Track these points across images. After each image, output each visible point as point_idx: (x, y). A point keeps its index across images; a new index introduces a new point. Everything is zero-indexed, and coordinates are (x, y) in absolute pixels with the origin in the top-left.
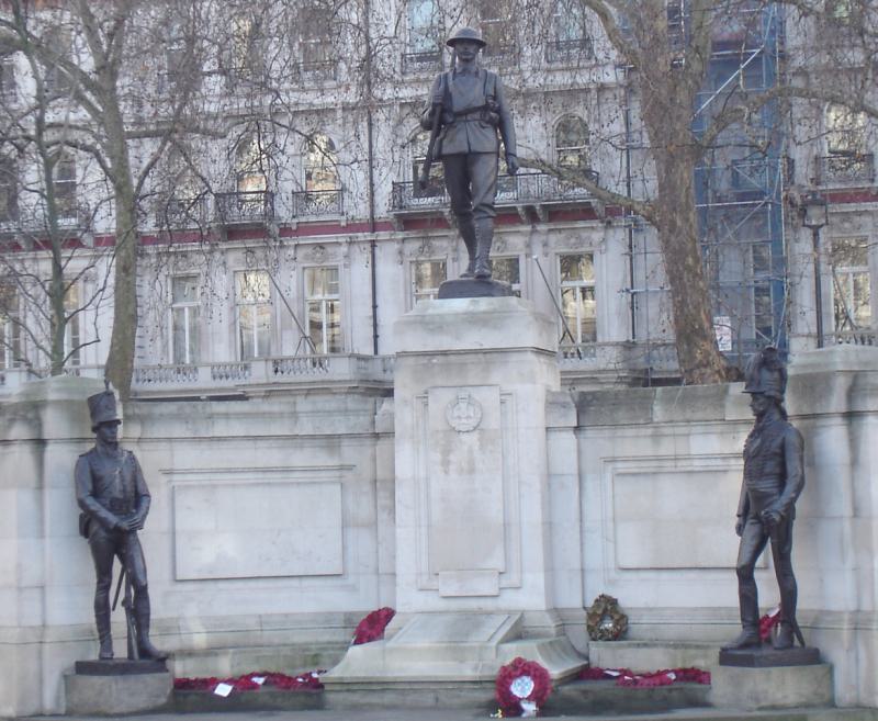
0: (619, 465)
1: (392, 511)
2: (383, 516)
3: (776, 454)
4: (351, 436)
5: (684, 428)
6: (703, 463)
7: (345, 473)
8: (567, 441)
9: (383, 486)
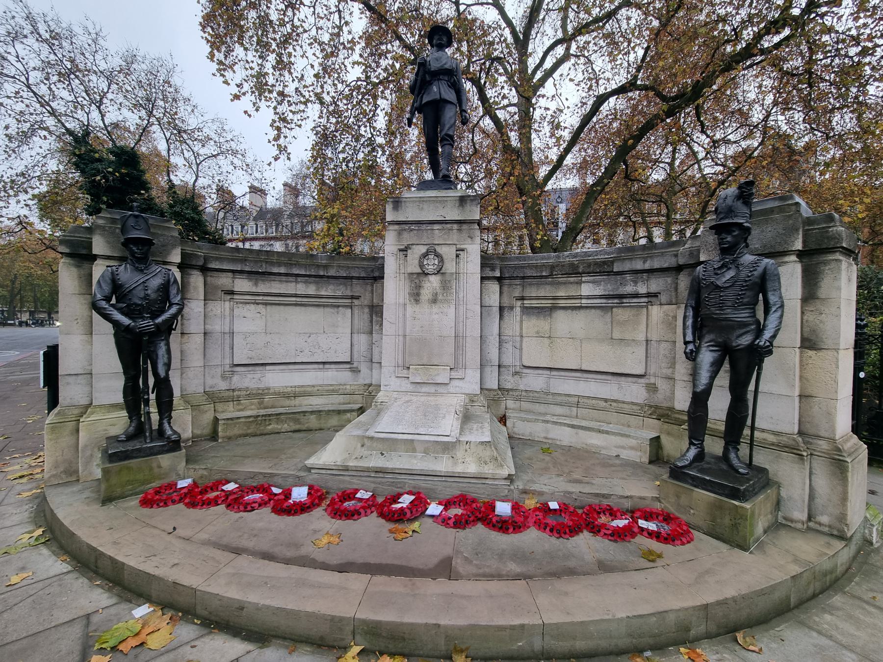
0: (525, 302)
1: (381, 325)
2: (376, 327)
3: (755, 283)
4: (358, 278)
6: (589, 301)
7: (354, 301)
8: (494, 287)
9: (376, 310)
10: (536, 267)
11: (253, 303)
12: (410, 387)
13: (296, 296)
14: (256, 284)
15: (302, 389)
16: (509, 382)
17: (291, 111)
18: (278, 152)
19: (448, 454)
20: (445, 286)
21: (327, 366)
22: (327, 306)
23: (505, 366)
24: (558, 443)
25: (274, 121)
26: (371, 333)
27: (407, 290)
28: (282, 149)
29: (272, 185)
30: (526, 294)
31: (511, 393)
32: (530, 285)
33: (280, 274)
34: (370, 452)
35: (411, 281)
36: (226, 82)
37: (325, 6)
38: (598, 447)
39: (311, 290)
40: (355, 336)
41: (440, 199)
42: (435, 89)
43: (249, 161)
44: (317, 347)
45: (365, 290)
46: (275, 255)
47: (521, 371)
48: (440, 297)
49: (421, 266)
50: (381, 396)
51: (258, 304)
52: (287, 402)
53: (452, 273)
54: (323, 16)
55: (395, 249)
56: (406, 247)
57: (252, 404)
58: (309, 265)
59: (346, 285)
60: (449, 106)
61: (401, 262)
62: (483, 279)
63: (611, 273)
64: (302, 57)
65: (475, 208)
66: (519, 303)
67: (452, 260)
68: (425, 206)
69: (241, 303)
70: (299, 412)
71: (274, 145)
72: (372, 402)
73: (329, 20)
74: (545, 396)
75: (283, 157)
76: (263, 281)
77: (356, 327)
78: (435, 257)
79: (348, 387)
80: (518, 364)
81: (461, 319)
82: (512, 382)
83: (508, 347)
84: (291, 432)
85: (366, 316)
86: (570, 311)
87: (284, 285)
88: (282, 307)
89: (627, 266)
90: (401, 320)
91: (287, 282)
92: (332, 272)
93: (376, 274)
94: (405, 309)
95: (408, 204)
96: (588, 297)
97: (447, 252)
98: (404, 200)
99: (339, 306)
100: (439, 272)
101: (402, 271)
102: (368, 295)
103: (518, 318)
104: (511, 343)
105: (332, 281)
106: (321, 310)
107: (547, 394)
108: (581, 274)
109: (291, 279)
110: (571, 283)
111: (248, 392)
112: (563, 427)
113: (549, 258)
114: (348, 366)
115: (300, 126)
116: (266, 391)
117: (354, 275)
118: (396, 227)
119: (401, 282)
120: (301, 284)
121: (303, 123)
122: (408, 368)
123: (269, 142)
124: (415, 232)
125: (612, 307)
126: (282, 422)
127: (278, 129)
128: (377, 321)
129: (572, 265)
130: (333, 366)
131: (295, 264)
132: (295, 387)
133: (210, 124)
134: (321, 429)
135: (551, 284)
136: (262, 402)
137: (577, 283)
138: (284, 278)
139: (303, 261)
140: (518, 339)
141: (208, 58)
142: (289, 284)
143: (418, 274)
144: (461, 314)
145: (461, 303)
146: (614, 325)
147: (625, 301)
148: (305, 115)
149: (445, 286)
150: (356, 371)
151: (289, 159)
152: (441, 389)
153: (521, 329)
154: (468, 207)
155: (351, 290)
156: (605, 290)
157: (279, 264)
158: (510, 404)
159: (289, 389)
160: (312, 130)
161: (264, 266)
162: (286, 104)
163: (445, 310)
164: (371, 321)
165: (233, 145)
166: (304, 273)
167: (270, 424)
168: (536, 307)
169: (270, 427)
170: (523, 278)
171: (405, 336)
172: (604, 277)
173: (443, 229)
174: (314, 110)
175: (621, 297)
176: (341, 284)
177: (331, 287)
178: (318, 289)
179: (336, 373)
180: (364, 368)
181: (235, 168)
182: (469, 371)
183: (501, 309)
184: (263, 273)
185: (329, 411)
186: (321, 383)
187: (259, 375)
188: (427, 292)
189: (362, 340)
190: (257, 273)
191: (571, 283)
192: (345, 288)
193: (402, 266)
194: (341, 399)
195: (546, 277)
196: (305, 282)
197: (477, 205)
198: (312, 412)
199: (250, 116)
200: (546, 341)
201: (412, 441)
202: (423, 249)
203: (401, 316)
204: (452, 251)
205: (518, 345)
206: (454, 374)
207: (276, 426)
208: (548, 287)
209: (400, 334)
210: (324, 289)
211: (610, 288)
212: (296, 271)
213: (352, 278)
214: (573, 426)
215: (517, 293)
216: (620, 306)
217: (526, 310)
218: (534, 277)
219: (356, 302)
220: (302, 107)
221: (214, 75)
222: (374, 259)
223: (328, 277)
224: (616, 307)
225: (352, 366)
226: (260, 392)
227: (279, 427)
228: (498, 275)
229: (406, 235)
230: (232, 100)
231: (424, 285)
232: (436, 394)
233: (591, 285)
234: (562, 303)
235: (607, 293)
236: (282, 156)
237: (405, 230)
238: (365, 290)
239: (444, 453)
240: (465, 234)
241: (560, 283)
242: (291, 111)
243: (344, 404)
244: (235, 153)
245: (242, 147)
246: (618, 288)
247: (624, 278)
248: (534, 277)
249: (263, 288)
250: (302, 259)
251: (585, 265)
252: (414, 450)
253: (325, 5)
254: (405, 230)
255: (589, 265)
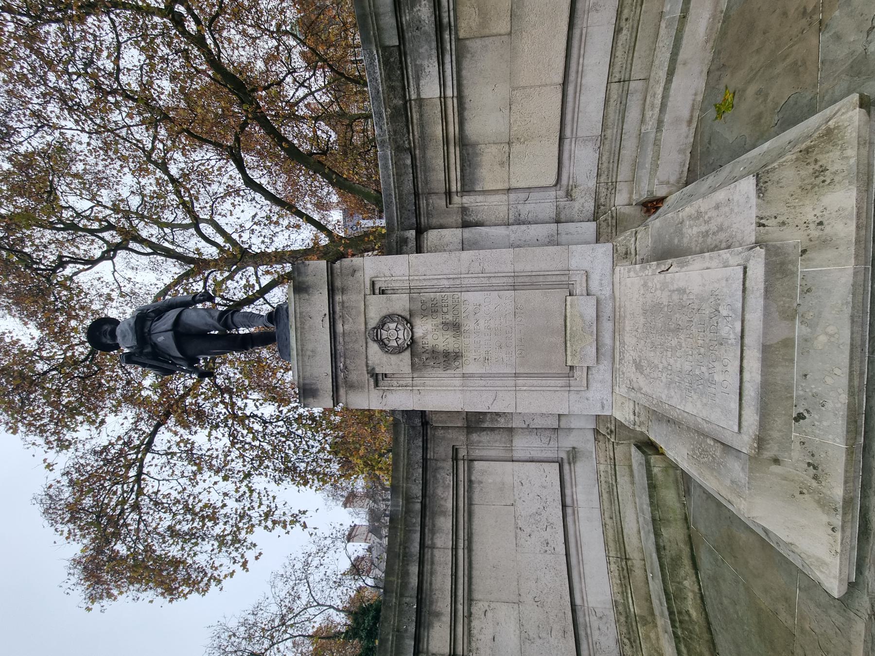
0: (454, 189)
1: (497, 414)
2: (502, 423)
4: (425, 449)
5: (414, 110)
6: (449, 83)
7: (460, 456)
8: (432, 236)
10: (399, 175)
11: (470, 622)
12: (605, 365)
13: (455, 549)
14: (438, 615)
15: (611, 544)
16: (584, 203)
17: (259, 507)
18: (298, 524)
19: (794, 263)
20: (431, 310)
21: (568, 501)
22: (470, 499)
23: (558, 214)
24: (700, 98)
25: (266, 527)
26: (511, 430)
27: (440, 372)
28: (295, 520)
29: (338, 527)
30: (441, 187)
31: (602, 200)
32: (427, 184)
33: (421, 574)
34: (796, 446)
35: (425, 366)
36: (232, 574)
37: (161, 468)
38: (714, 16)
39: (445, 523)
40: (517, 455)
41: (298, 325)
42: (161, 339)
43: (314, 550)
44: (538, 518)
45: (443, 438)
46: (391, 579)
47: (564, 188)
48: (450, 317)
49: (399, 350)
50: (624, 414)
51: (470, 614)
52: (638, 573)
53: (411, 299)
54: (171, 471)
55: (375, 394)
56: (372, 376)
57: (647, 637)
58: (406, 526)
59: (436, 470)
60: (184, 317)
61: (395, 383)
62: (419, 250)
63: (402, 49)
64: (209, 492)
65: (310, 268)
66: (456, 199)
67: (389, 300)
68: (309, 346)
69: (469, 643)
70: (660, 558)
71: (292, 528)
72: (633, 431)
73: (175, 464)
74: (607, 142)
75: (303, 519)
76: (431, 603)
77: (502, 454)
78: (386, 327)
79: (602, 468)
80: (553, 193)
81: (485, 281)
82: (583, 200)
83: (526, 210)
84: (697, 574)
85: (485, 437)
86: (466, 113)
87: (439, 569)
88: (475, 573)
89: (388, 20)
90: (490, 382)
91: (432, 563)
92: (417, 490)
93: (418, 422)
94: (472, 376)
95: (308, 374)
96: (443, 85)
97: (377, 308)
98: (301, 380)
99: (470, 481)
100: (408, 321)
101: (409, 381)
102: (451, 434)
103: (480, 198)
104: (520, 207)
105: (430, 491)
106: (477, 509)
107: (603, 138)
108: (406, 102)
109: (428, 556)
110: (421, 116)
111: (626, 641)
112: (672, 92)
113: (385, 158)
114: (566, 467)
115: (274, 498)
116: (620, 608)
117: (420, 455)
118: (342, 392)
119: (428, 382)
120: (435, 541)
121: (272, 494)
122: (572, 368)
123: (288, 533)
124: (348, 362)
125: (458, 40)
126: (681, 590)
127: (274, 522)
128: (492, 421)
129: (393, 118)
130: (568, 492)
131: (405, 548)
132: (608, 556)
133: (277, 590)
134: (686, 519)
135: (424, 148)
136: (643, 618)
137: (420, 106)
138: (427, 567)
139: (400, 535)
140: (513, 196)
141: (204, 595)
142: (437, 559)
143: (413, 355)
144: (477, 281)
145: (458, 282)
146: (487, 32)
147: (446, 20)
148: (263, 492)
149: (431, 310)
150: (574, 455)
151: (304, 512)
152: (607, 311)
153: (496, 192)
154: (309, 279)
155: (444, 460)
156: (430, 56)
157: (405, 574)
158: (621, 199)
159: (613, 567)
160: (279, 484)
161: (408, 600)
162: (251, 512)
163: (471, 308)
164: (492, 429)
165: (299, 565)
166: (418, 535)
167: (687, 612)
168: (462, 171)
169: (694, 614)
170: (416, 195)
171: (516, 375)
172: (409, 61)
173: (342, 317)
174: (259, 482)
175: (439, 27)
176: (435, 476)
177: (439, 491)
178: (444, 513)
179: (580, 488)
180: (568, 442)
181: (321, 565)
182: (574, 264)
183: (466, 225)
184: (420, 602)
185: (652, 504)
186: (597, 514)
187: (593, 618)
188: (441, 339)
189: (523, 445)
190: (419, 611)
191: (421, 116)
192: (441, 471)
193: (401, 382)
194: (623, 480)
195: (414, 158)
196: (433, 532)
197: (305, 266)
198: (657, 534)
199: (260, 554)
200: (516, 148)
201: (766, 350)
202: (374, 347)
203: (482, 383)
204: (374, 300)
205: (522, 196)
206: (579, 289)
207: (690, 602)
208: (430, 153)
209: (513, 383)
210: (442, 502)
211: (426, 47)
212: (415, 548)
213: (425, 459)
214: (671, 73)
215: (441, 202)
216: (454, 28)
217: (467, 188)
218: (415, 178)
219: (462, 453)
220: (255, 495)
221: (221, 589)
222: (396, 424)
223: (424, 496)
224: (456, 34)
225: (566, 461)
226: (623, 619)
227: (690, 595)
228: (413, 232)
229: (353, 377)
230: (247, 571)
231: (430, 345)
232: (615, 319)
233: (422, 82)
234: (453, 129)
235: (434, 52)
236: (302, 520)
237: (345, 378)
238: (443, 438)
239: (794, 274)
240: (350, 282)
241: (423, 136)
242: (259, 507)
243: (632, 475)
244: (307, 564)
245: (300, 556)
246: (425, 33)
247: (409, 25)
248: (415, 178)
249: (443, 604)
250: (396, 535)
251: (391, 96)
252: (787, 343)
253: (161, 468)
254: (345, 378)
255: (392, 88)
